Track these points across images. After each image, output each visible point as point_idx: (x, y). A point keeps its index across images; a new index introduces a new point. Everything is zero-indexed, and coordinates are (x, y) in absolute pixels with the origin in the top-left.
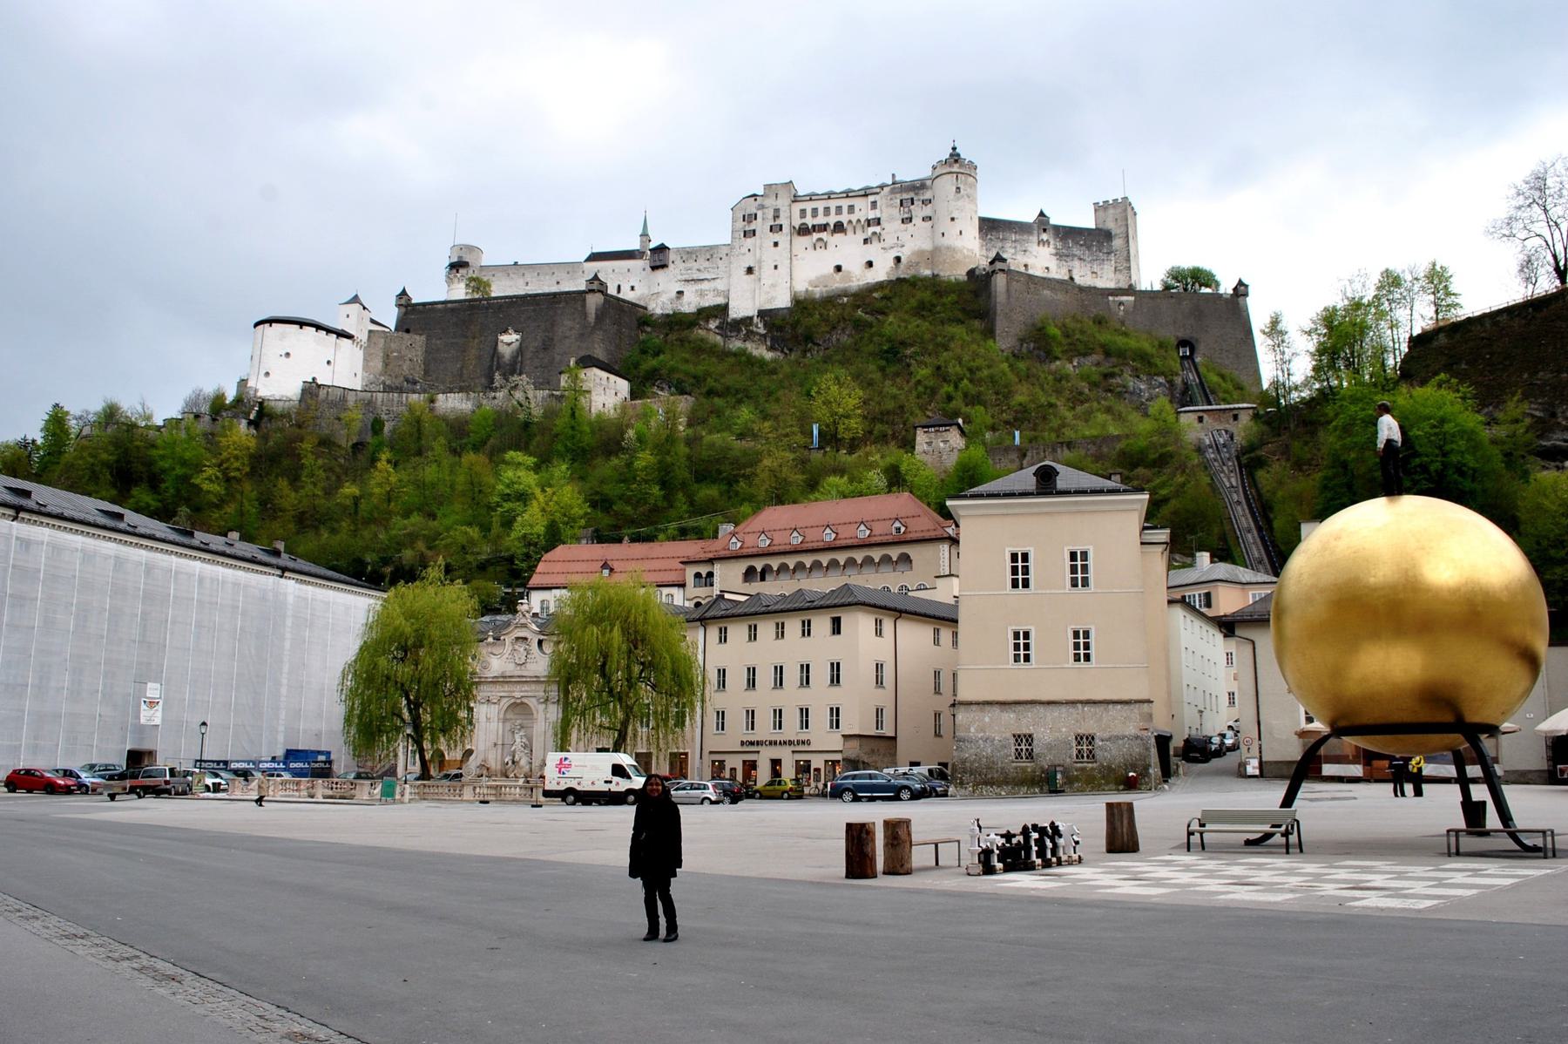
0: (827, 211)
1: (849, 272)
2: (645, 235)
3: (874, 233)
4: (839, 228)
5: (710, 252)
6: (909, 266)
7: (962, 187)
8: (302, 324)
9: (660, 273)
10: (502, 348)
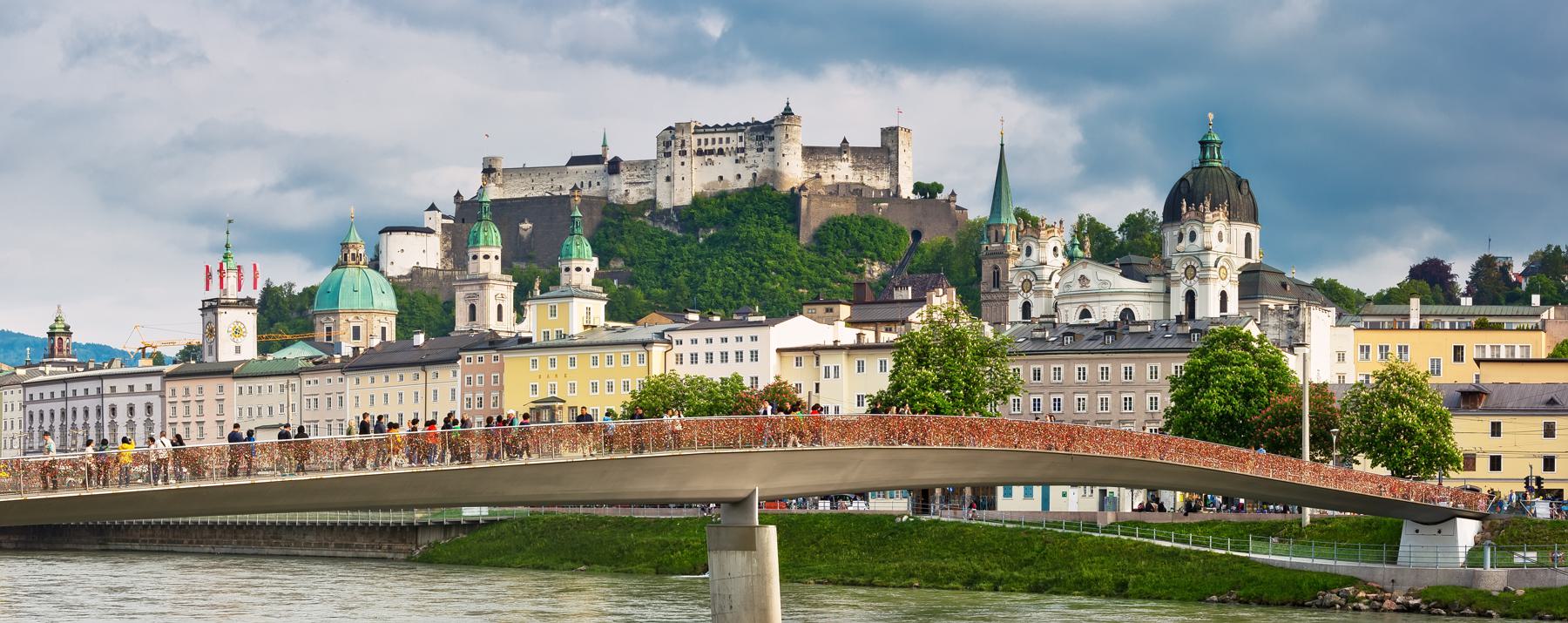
0: (714, 140)
1: (727, 181)
2: (604, 145)
3: (741, 157)
4: (721, 152)
5: (645, 165)
6: (761, 180)
7: (789, 134)
8: (408, 230)
9: (614, 179)
10: (521, 232)
